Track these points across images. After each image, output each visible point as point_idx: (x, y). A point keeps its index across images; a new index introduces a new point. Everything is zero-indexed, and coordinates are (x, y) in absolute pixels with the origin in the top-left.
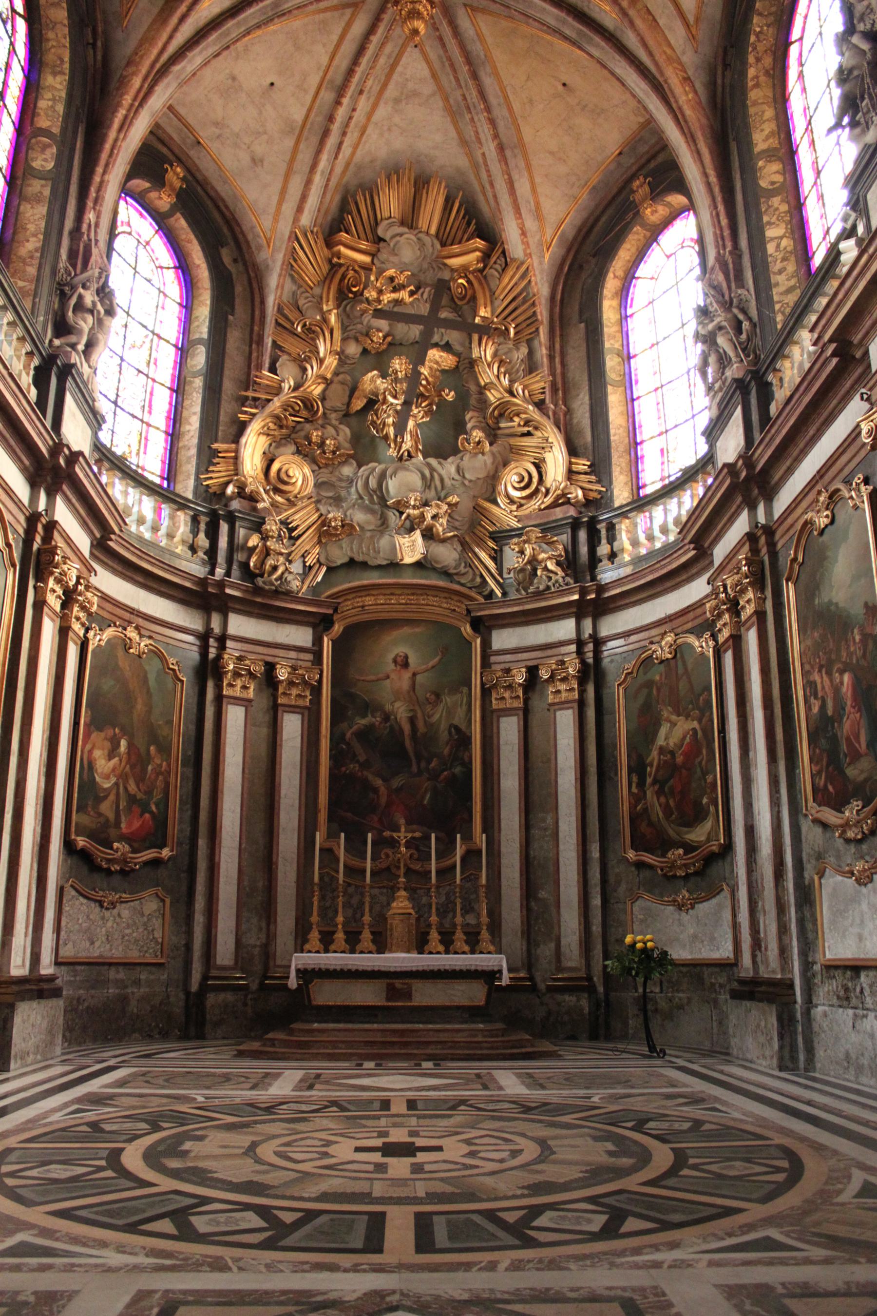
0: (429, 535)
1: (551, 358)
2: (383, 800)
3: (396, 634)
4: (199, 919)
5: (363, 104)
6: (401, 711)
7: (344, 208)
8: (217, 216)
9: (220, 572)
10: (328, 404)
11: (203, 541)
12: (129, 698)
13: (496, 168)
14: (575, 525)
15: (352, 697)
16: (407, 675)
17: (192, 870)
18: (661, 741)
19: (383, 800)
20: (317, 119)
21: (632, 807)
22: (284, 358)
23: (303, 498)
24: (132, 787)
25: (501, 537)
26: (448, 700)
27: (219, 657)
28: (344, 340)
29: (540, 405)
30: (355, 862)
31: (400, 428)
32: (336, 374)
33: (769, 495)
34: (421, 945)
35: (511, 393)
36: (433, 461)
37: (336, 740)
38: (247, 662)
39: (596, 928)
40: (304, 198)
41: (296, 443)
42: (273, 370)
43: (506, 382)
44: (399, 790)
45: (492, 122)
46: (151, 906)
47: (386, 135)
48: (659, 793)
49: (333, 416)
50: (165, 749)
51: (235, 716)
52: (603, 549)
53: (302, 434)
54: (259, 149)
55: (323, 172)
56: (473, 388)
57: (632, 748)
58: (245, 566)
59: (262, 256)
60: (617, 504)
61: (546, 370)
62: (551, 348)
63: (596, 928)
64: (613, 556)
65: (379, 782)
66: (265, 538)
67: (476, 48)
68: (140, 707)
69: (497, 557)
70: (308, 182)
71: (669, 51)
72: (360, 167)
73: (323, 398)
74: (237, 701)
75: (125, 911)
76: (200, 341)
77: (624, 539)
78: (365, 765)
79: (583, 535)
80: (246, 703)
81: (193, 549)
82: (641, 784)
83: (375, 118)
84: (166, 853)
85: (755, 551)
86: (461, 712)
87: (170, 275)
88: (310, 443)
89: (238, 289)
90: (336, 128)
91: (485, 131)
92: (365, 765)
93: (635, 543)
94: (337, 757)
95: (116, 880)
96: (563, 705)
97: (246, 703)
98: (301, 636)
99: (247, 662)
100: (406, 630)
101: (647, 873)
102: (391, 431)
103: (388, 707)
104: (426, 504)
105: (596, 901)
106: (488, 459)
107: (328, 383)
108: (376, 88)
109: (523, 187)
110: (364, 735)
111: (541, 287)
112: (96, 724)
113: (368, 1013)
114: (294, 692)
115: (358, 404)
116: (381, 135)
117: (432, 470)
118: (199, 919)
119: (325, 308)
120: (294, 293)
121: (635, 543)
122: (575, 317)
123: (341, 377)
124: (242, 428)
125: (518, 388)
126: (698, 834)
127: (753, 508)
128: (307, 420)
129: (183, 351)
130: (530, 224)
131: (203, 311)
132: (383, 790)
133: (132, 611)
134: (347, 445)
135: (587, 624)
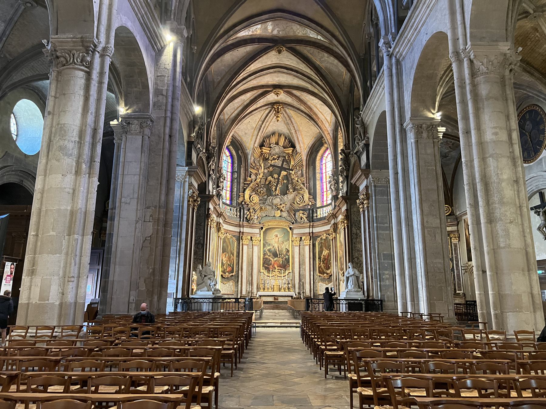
0: (281, 211)
1: (306, 173)
2: (273, 263)
3: (275, 230)
4: (240, 286)
6: (276, 246)
7: (264, 141)
8: (238, 144)
9: (242, 220)
11: (238, 214)
12: (228, 247)
13: (294, 135)
14: (309, 209)
15: (267, 243)
16: (277, 238)
17: (238, 277)
18: (323, 254)
19: (273, 263)
20: (258, 127)
21: (319, 265)
24: (228, 263)
25: (296, 211)
26: (285, 243)
27: (242, 237)
28: (264, 169)
29: (303, 184)
30: (268, 275)
31: (276, 190)
32: (263, 176)
33: (337, 218)
34: (280, 290)
35: (298, 181)
36: (282, 196)
37: (264, 251)
39: (312, 288)
40: (255, 141)
42: (250, 177)
43: (297, 179)
44: (276, 261)
45: (294, 127)
46: (231, 284)
48: (323, 263)
50: (233, 255)
51: (245, 247)
52: (315, 215)
54: (246, 132)
56: (290, 179)
57: (319, 254)
58: (246, 218)
59: (248, 151)
60: (318, 206)
61: (305, 176)
62: (306, 171)
63: (312, 288)
64: (316, 216)
65: (272, 259)
66: (250, 213)
67: (290, 115)
68: (229, 248)
69: (295, 215)
70: (256, 138)
71: (325, 128)
72: (267, 133)
73: (260, 182)
74: (246, 245)
75: (227, 285)
76: (236, 172)
77: (319, 213)
78: (269, 256)
79: (311, 211)
80: (247, 245)
81: (236, 215)
82: (320, 261)
84: (234, 274)
85: (334, 226)
86: (287, 245)
87: (229, 157)
89: (242, 159)
90: (262, 128)
91: (292, 128)
92: (269, 256)
93: (320, 214)
94: (264, 255)
95: (226, 279)
96: (307, 245)
97: (247, 245)
98: (257, 231)
100: (277, 229)
101: (321, 278)
102: (274, 190)
103: (274, 245)
104: (281, 205)
105: (312, 283)
106: (293, 195)
107: (261, 179)
109: (300, 138)
110: (269, 250)
111: (304, 158)
112: (223, 252)
113: (271, 302)
115: (267, 183)
117: (282, 198)
118: (240, 286)
120: (254, 160)
121: (320, 214)
122: (311, 165)
124: (244, 190)
125: (299, 180)
126: (328, 272)
127: (334, 219)
129: (232, 173)
130: (302, 145)
131: (236, 165)
132: (273, 261)
133: (228, 230)
135: (311, 229)
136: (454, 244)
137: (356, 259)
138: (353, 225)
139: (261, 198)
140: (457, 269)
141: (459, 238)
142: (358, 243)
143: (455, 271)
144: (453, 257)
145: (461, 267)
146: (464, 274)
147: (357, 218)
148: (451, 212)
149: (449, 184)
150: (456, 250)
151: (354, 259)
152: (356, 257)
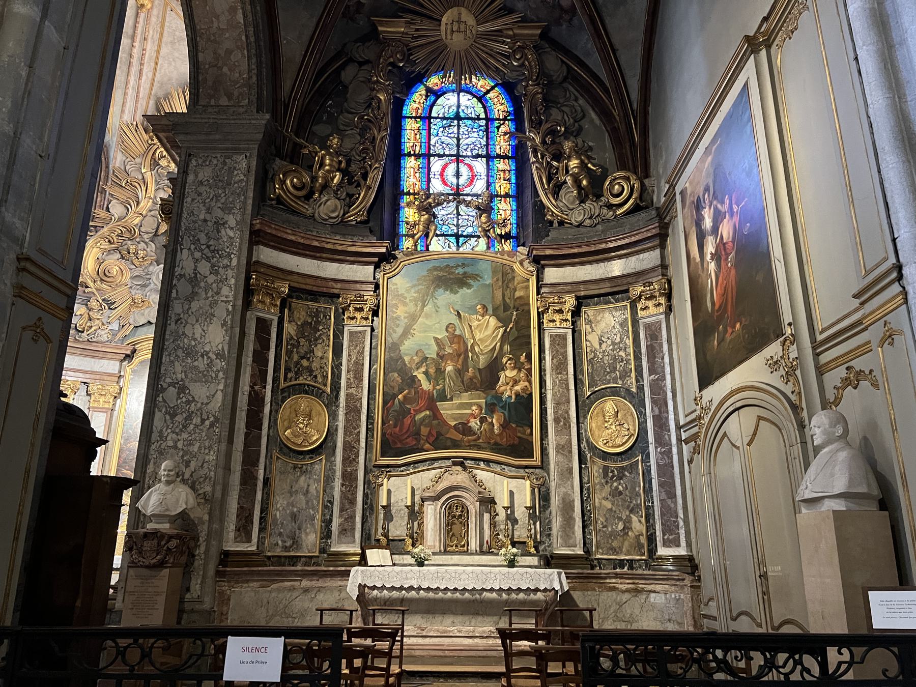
5: (150, 47)
10: (143, 229)
22: (114, 201)
23: (121, 285)
38: (69, 382)
41: (120, 253)
47: (173, 64)
49: (146, 236)
53: (126, 247)
55: (133, 88)
83: (161, 54)
88: (129, 253)
99: (69, 382)
108: (157, 36)
114: (102, 399)
116: (170, 64)
119: (143, 171)
123: (152, 213)
128: (130, 239)
134: (153, 254)
136: (648, 327)
137: (172, 391)
138: (187, 242)
139: (139, 271)
140: (661, 441)
141: (669, 296)
142: (192, 320)
143: (652, 448)
144: (641, 388)
145: (679, 427)
146: (690, 462)
147: (209, 211)
148: (641, 197)
149: (635, 95)
150: (653, 352)
151: (164, 390)
152: (172, 384)
